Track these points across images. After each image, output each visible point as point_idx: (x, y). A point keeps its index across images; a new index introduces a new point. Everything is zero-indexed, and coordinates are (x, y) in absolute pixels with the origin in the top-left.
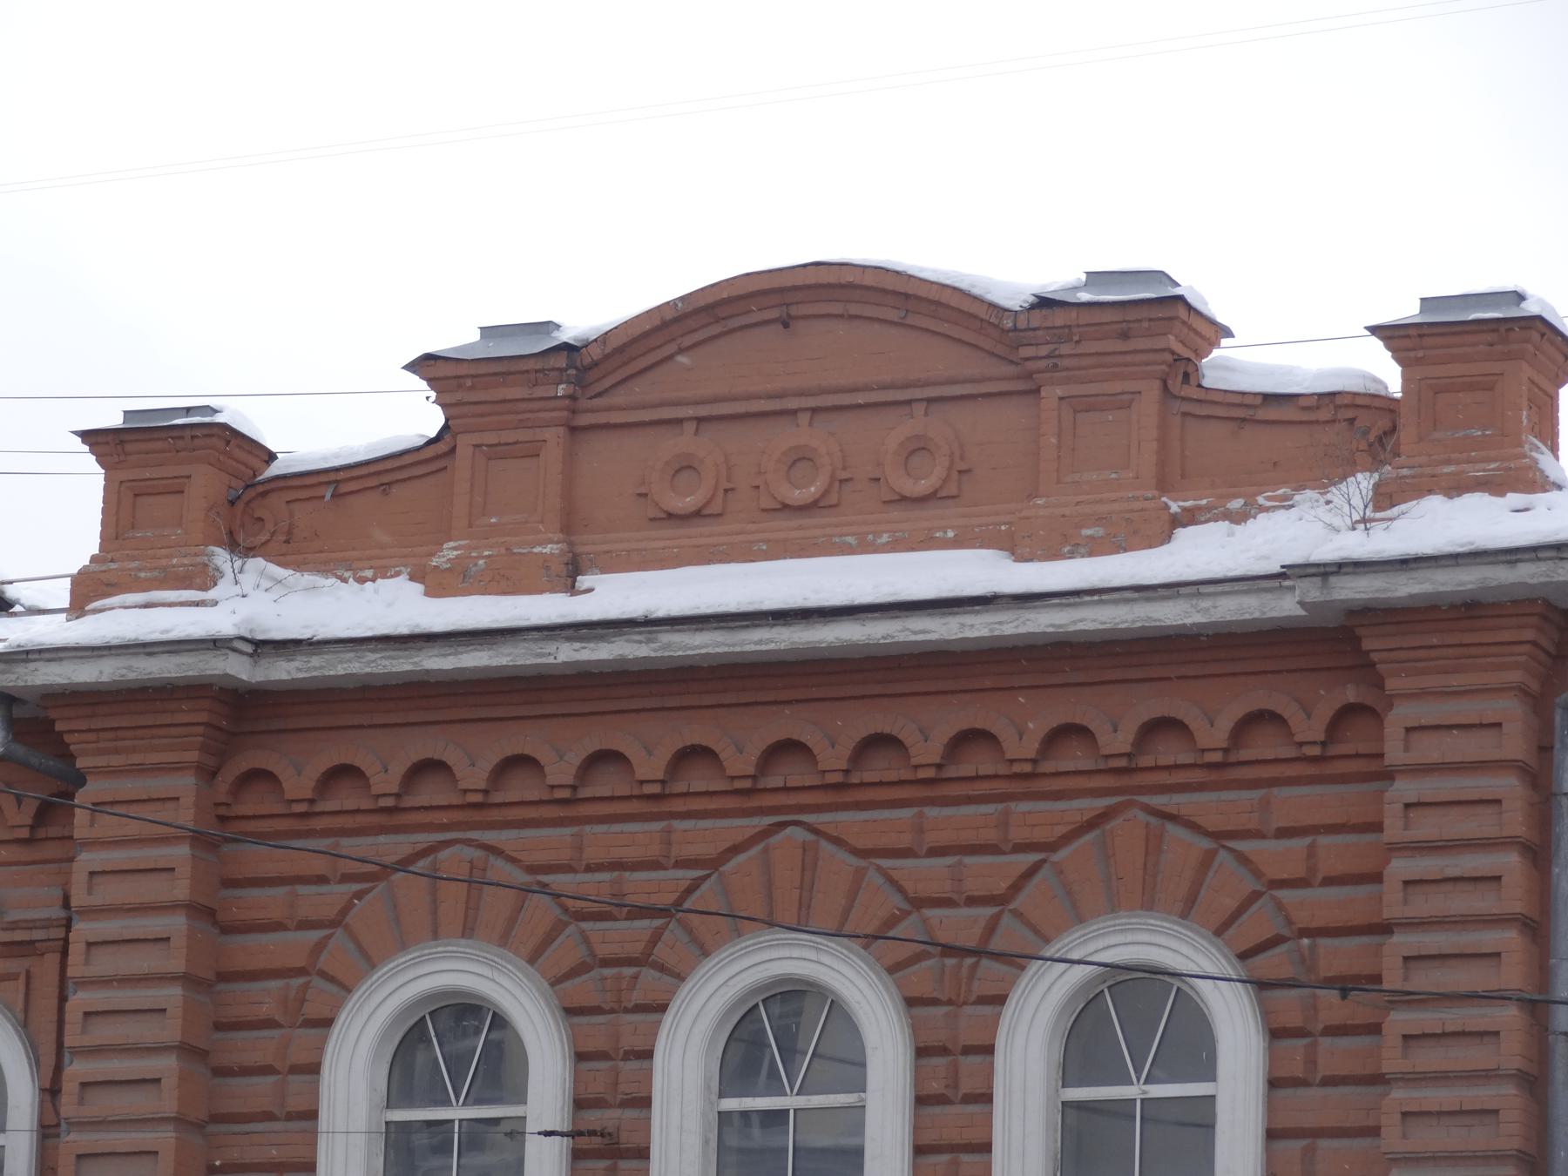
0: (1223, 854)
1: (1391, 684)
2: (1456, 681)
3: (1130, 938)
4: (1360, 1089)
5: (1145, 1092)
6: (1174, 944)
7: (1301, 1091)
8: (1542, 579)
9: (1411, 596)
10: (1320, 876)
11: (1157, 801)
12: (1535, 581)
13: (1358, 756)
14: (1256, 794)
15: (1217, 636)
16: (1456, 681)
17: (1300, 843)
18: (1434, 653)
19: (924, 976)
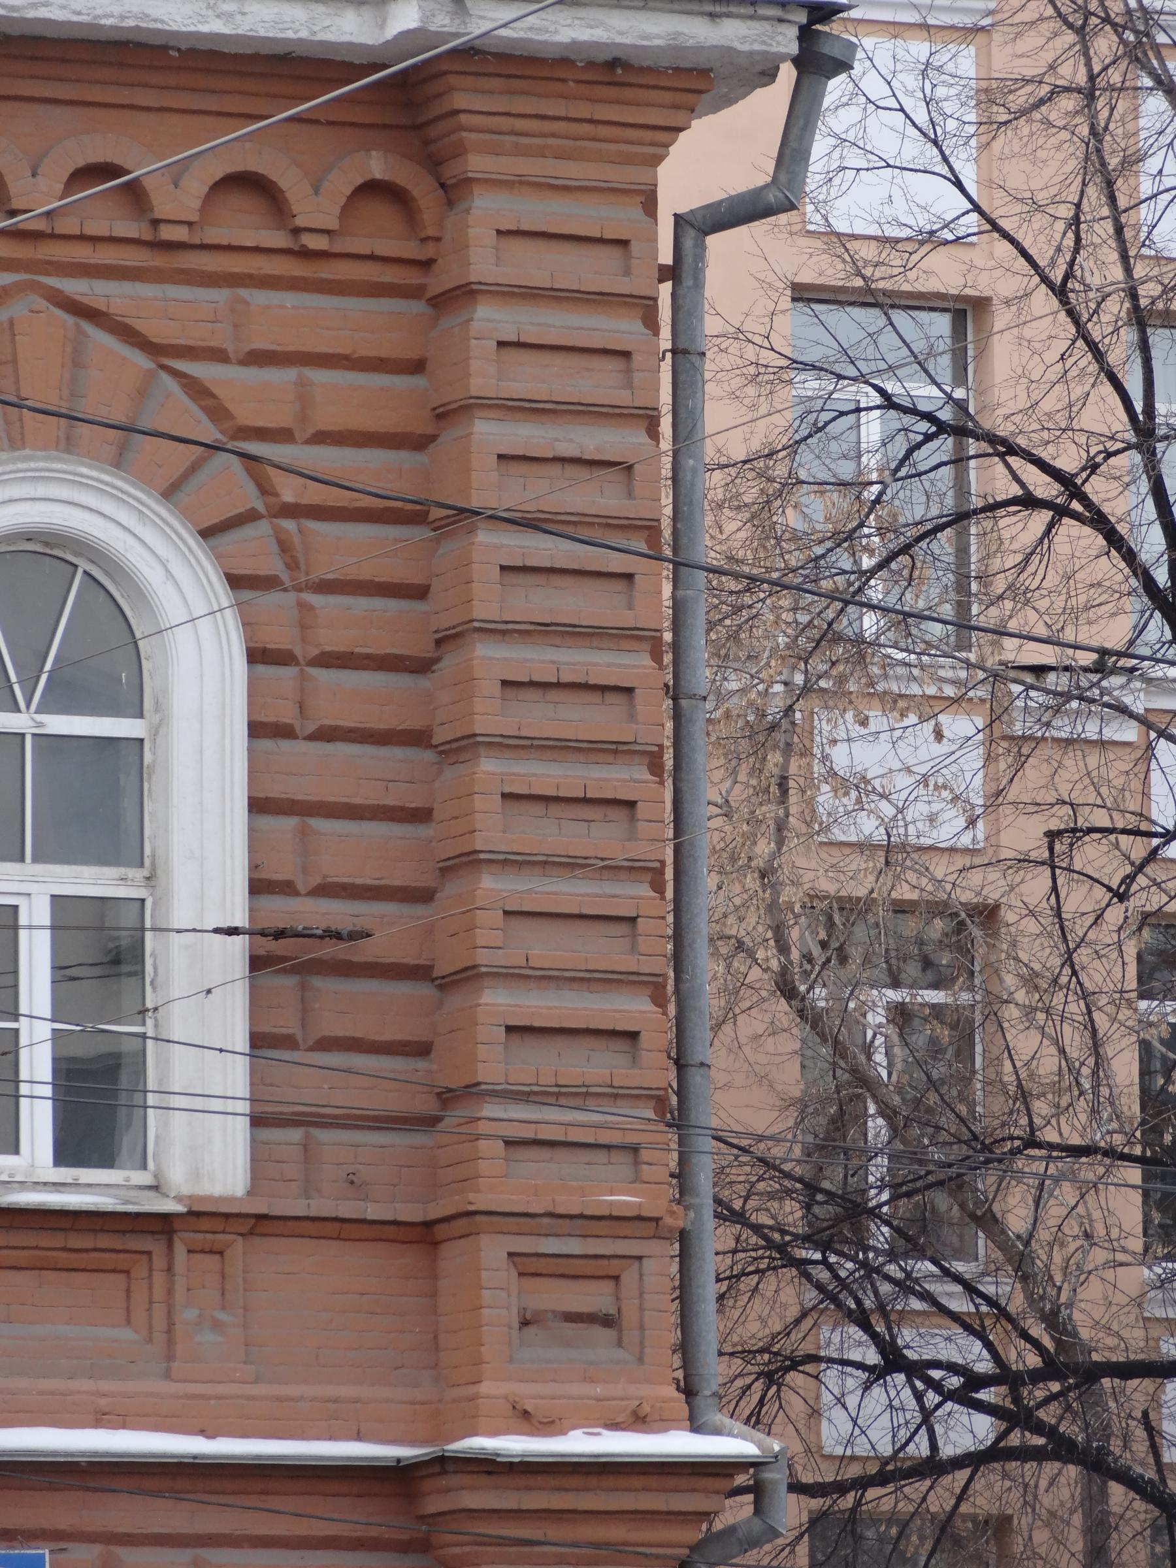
0: (165, 377)
1: (477, 163)
2: (573, 171)
3: (42, 490)
4: (369, 750)
5: (40, 725)
6: (108, 507)
7: (285, 745)
8: (757, 47)
9: (574, 43)
10: (310, 431)
11: (75, 287)
12: (746, 48)
13: (372, 257)
14: (220, 296)
15: (192, 52)
16: (573, 171)
17: (284, 377)
18: (548, 126)
19: (255, 546)
